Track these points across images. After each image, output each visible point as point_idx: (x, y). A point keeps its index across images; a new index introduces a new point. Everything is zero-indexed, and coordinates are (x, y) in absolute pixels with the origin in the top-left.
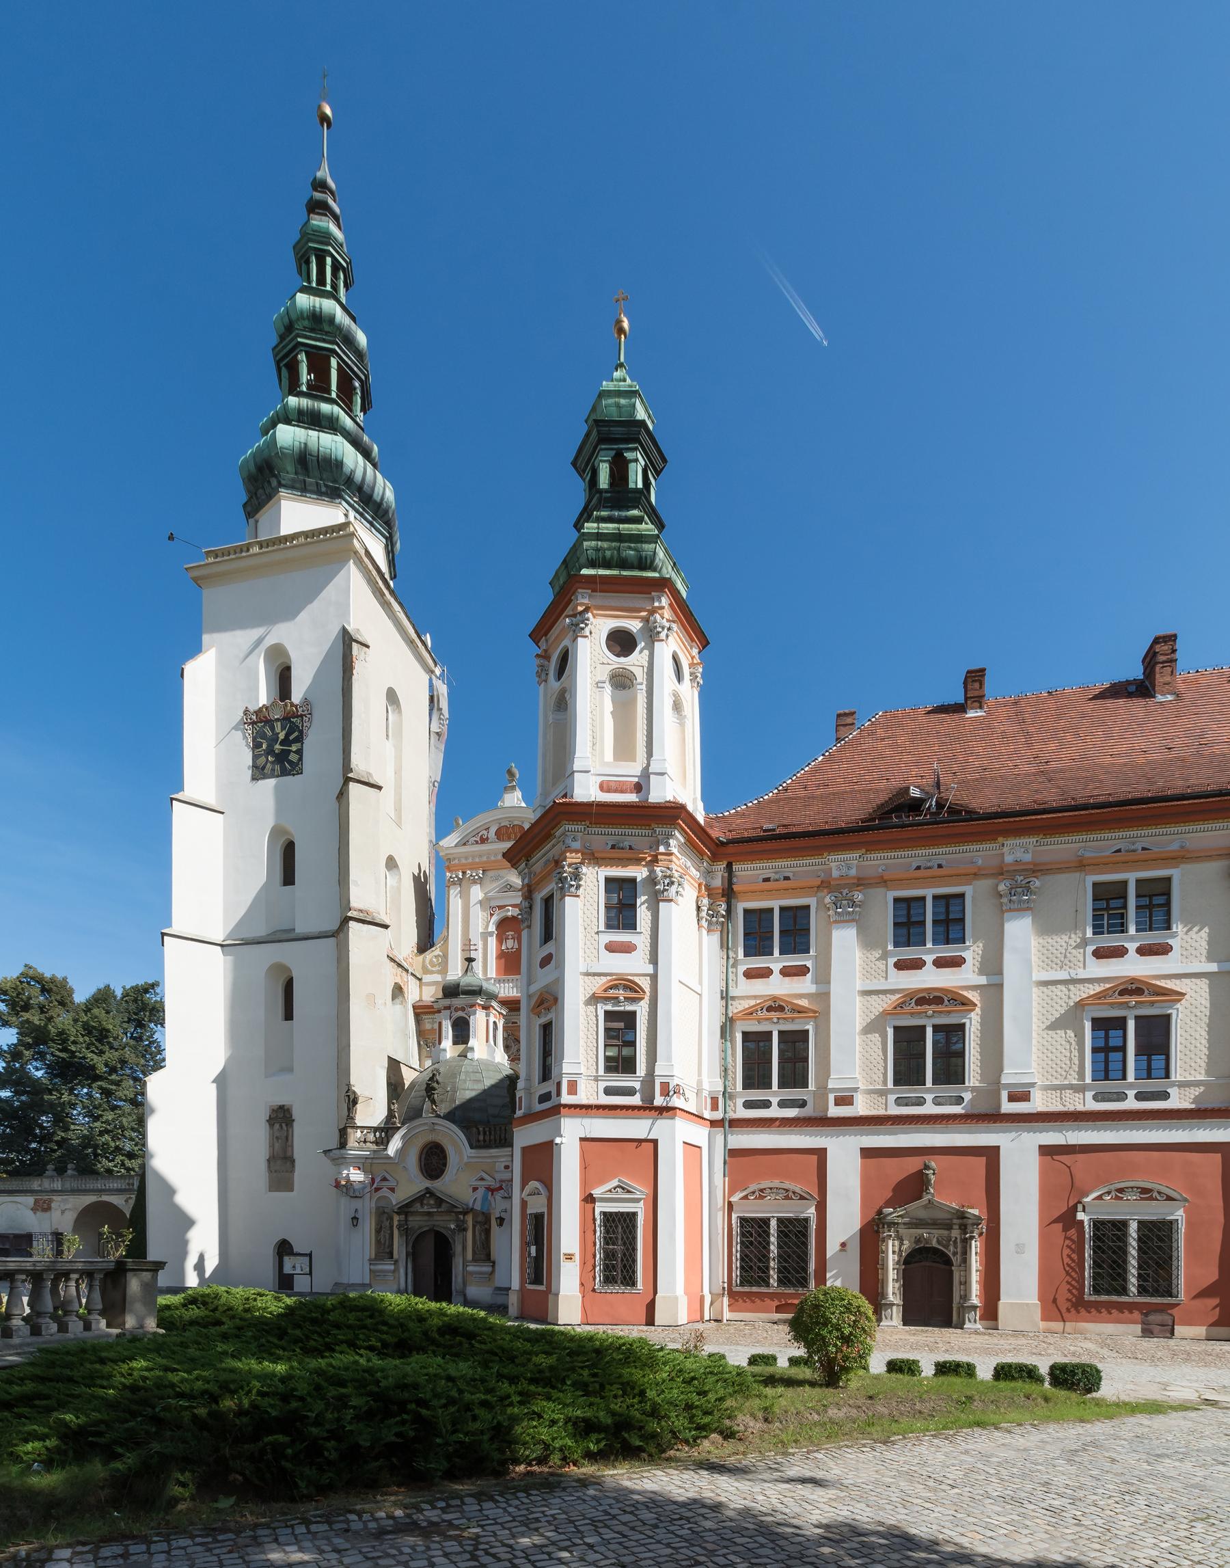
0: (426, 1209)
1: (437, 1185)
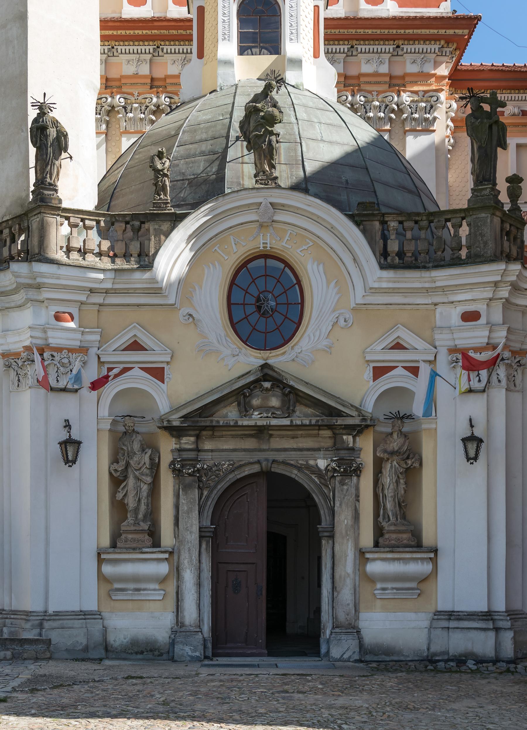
0: (256, 418)
1: (281, 359)
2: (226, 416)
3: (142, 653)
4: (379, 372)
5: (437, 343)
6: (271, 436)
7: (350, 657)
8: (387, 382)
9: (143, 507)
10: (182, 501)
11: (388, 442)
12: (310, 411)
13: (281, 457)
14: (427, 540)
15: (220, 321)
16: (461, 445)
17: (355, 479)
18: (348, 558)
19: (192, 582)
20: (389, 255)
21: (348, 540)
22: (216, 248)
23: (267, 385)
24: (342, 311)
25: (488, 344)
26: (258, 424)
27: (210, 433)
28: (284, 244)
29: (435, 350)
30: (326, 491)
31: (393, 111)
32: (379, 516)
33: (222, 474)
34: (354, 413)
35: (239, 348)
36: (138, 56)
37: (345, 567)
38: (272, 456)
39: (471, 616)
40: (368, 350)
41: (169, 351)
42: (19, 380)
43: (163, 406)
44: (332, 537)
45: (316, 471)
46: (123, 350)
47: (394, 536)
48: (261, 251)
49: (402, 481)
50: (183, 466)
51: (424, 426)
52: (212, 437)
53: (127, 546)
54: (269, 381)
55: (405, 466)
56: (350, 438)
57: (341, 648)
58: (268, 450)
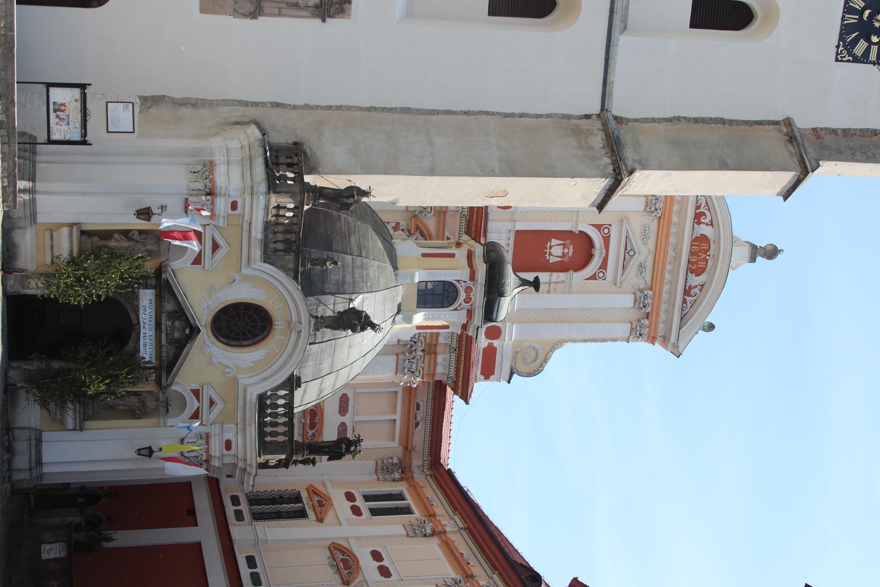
1: (206, 336)
2: (169, 303)
4: (196, 393)
12: (172, 354)
23: (187, 331)
31: (412, 346)
34: (169, 382)
39: (39, 453)
51: (161, 420)
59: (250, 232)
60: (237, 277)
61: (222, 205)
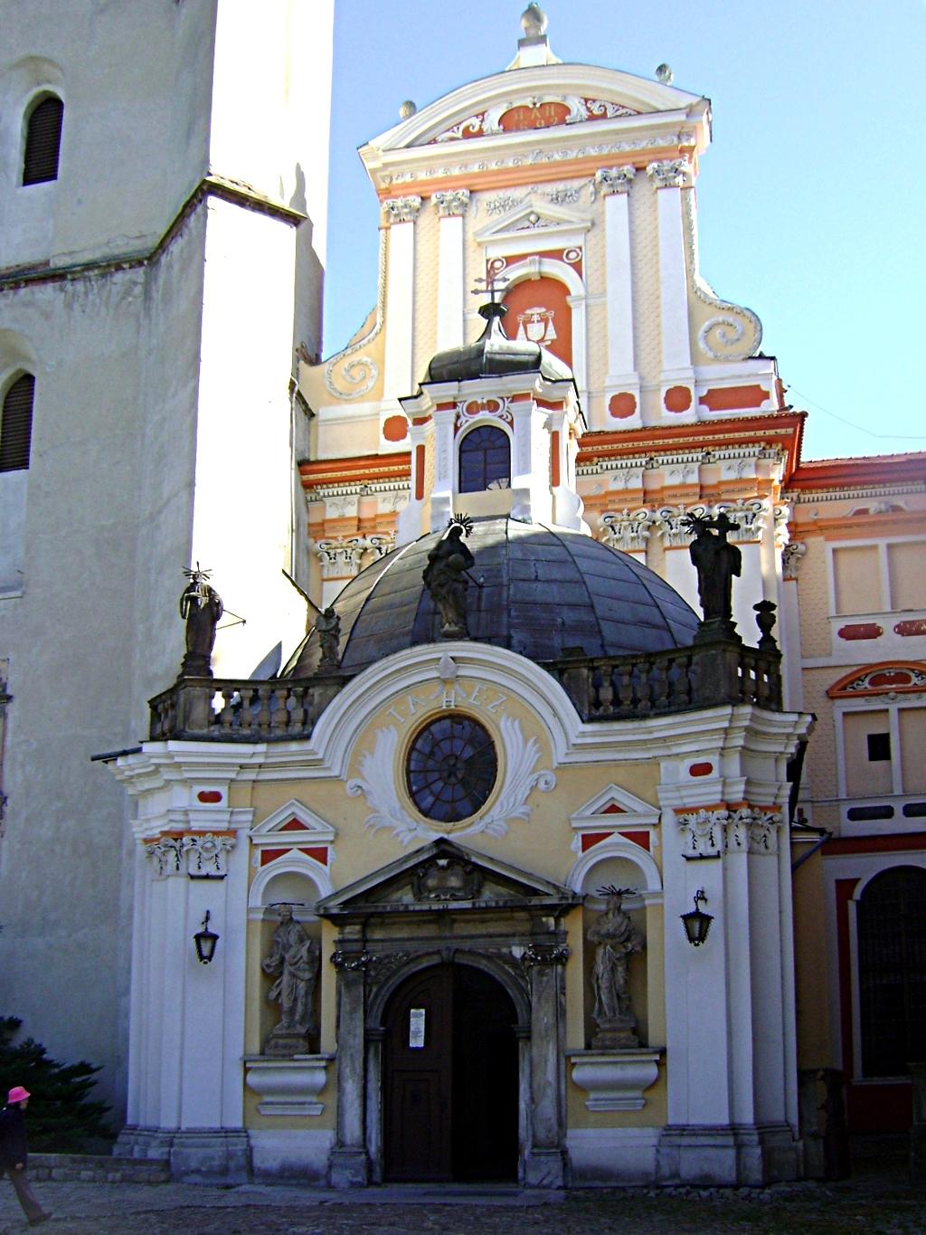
1: (465, 834)
2: (400, 900)
3: (295, 1178)
4: (589, 841)
5: (661, 803)
6: (454, 921)
7: (552, 1183)
8: (599, 852)
9: (300, 1008)
10: (345, 999)
11: (602, 923)
13: (466, 945)
14: (654, 1038)
15: (394, 792)
16: (681, 922)
17: (559, 967)
18: (548, 1063)
19: (355, 1093)
20: (602, 705)
21: (549, 1041)
22: (391, 710)
23: (443, 862)
24: (542, 772)
25: (722, 800)
26: (433, 908)
27: (379, 920)
28: (471, 700)
29: (658, 812)
30: (523, 984)
32: (593, 1010)
33: (394, 967)
34: (551, 891)
35: (417, 822)
36: (395, 492)
37: (545, 1074)
38: (455, 944)
40: (574, 815)
41: (331, 829)
42: (161, 868)
43: (325, 890)
44: (529, 1038)
45: (510, 959)
46: (280, 830)
47: (609, 1035)
48: (444, 711)
49: (620, 969)
50: (345, 960)
52: (382, 925)
53: (277, 1053)
54: (446, 858)
55: (623, 950)
56: (552, 921)
57: (538, 1172)
58: (450, 938)
59: (260, 766)
60: (351, 783)
61: (207, 818)
